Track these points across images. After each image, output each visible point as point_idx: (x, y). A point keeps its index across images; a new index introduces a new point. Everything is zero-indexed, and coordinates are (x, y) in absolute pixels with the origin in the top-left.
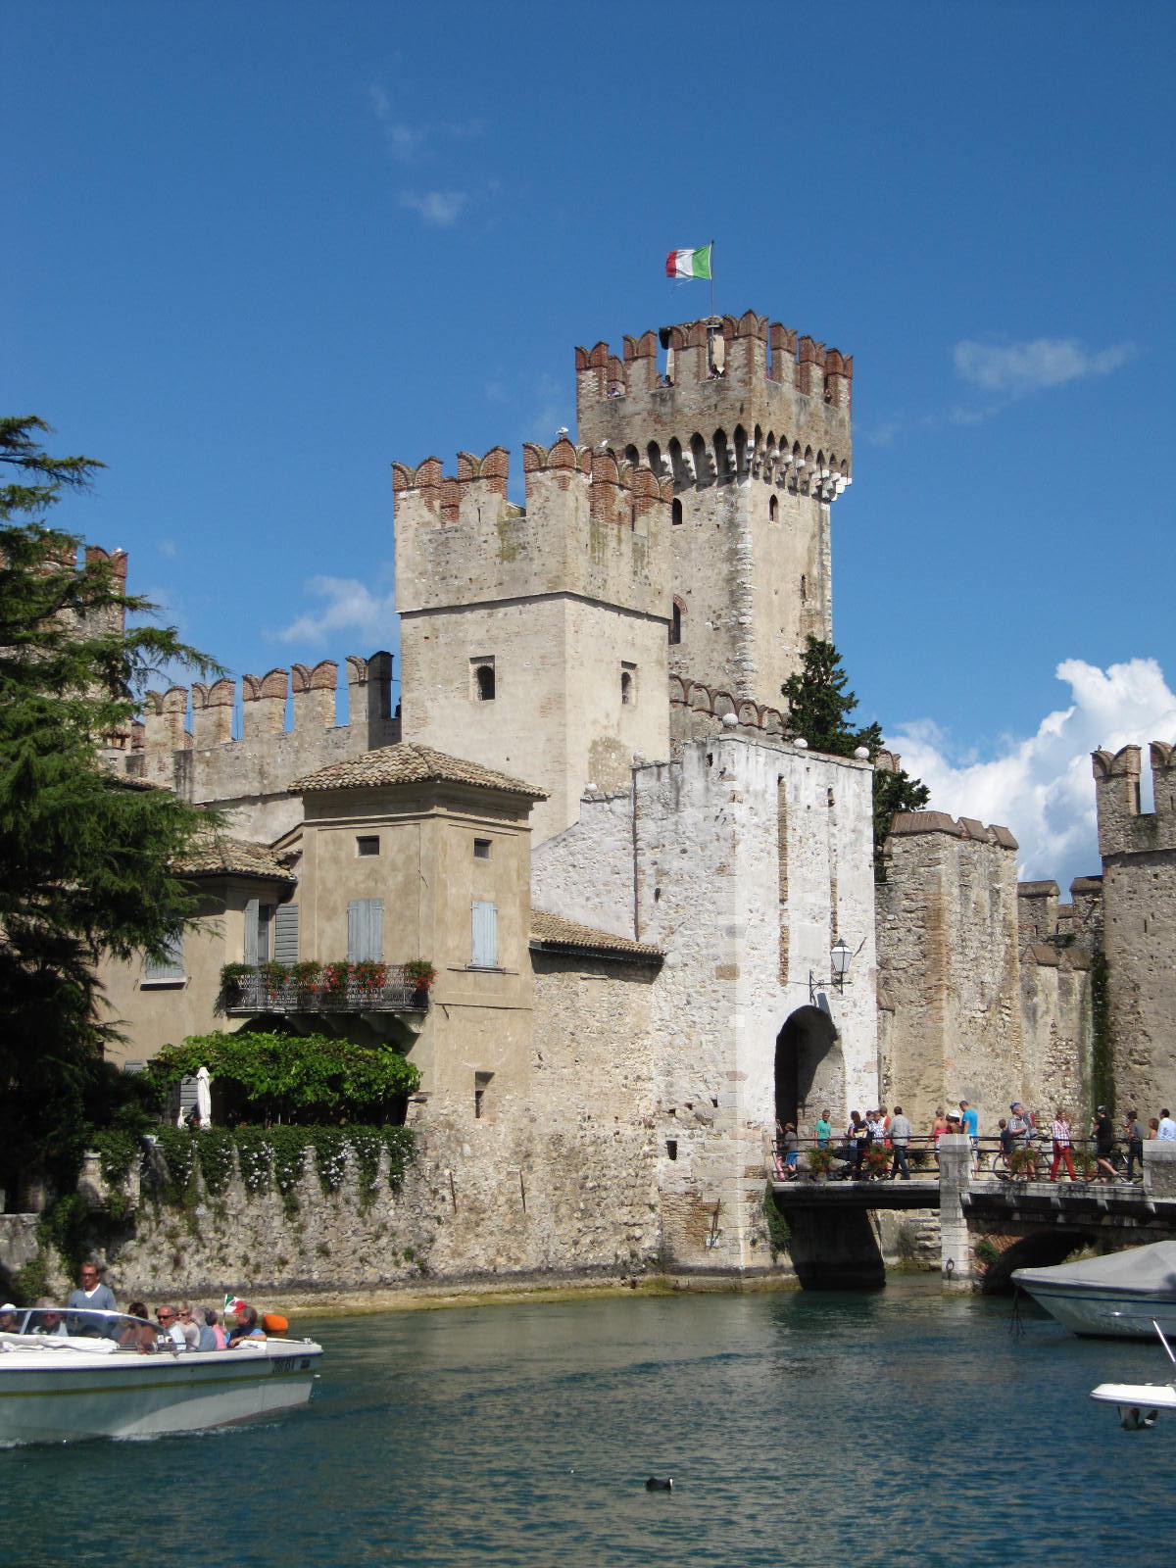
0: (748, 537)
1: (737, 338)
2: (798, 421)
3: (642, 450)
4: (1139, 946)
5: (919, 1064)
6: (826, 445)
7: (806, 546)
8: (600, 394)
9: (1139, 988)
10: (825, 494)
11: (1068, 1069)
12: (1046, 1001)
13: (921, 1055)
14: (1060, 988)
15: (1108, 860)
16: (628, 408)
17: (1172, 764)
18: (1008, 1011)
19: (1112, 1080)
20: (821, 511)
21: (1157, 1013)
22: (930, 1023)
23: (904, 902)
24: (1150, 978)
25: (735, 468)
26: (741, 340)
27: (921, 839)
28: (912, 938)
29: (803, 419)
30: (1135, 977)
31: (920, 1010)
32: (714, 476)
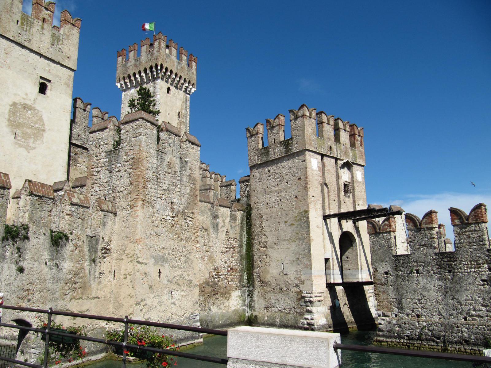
0: (158, 96)
1: (156, 40)
2: (177, 67)
3: (132, 75)
4: (263, 200)
5: (125, 242)
6: (187, 77)
7: (181, 104)
8: (123, 63)
9: (263, 217)
10: (188, 92)
11: (234, 250)
12: (224, 222)
13: (126, 237)
14: (231, 217)
15: (251, 168)
16: (129, 64)
17: (274, 126)
18: (191, 219)
19: (253, 254)
20: (186, 96)
21: (269, 226)
22: (132, 220)
23: (125, 157)
24: (267, 212)
25: (156, 76)
26: (158, 40)
27: (133, 124)
28: (127, 175)
29: (179, 68)
30: (261, 212)
31: (128, 212)
32: (150, 80)
